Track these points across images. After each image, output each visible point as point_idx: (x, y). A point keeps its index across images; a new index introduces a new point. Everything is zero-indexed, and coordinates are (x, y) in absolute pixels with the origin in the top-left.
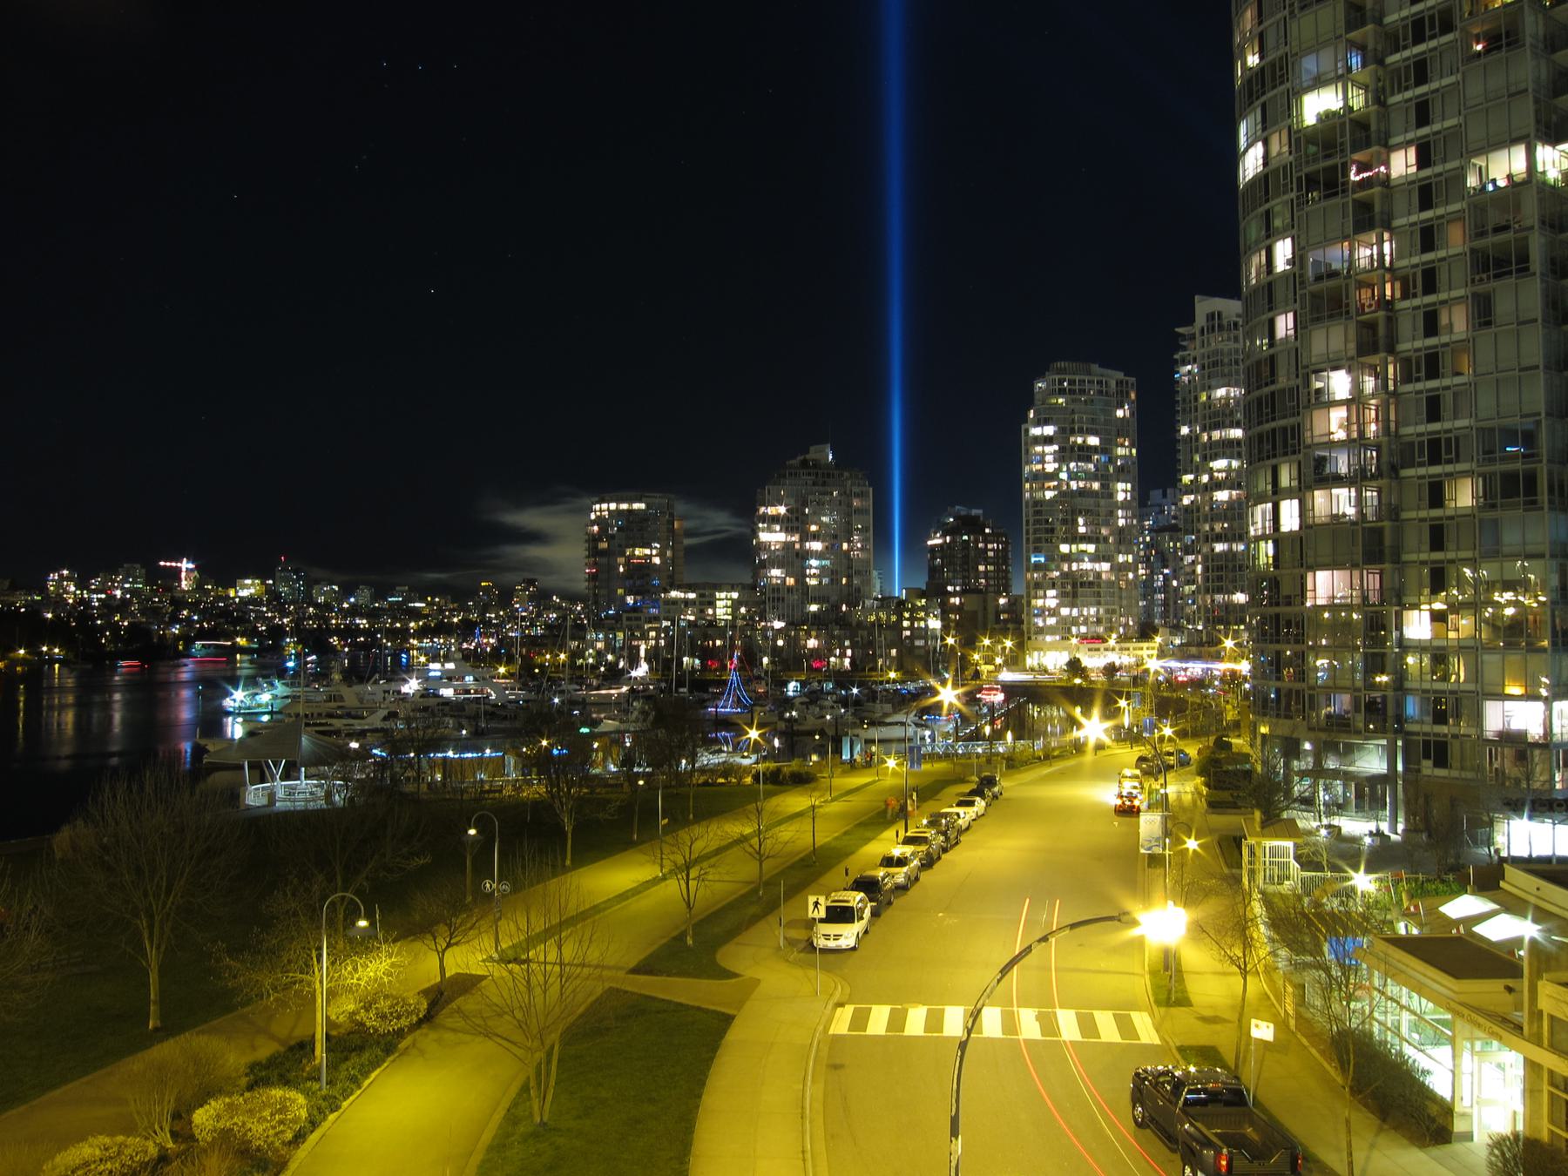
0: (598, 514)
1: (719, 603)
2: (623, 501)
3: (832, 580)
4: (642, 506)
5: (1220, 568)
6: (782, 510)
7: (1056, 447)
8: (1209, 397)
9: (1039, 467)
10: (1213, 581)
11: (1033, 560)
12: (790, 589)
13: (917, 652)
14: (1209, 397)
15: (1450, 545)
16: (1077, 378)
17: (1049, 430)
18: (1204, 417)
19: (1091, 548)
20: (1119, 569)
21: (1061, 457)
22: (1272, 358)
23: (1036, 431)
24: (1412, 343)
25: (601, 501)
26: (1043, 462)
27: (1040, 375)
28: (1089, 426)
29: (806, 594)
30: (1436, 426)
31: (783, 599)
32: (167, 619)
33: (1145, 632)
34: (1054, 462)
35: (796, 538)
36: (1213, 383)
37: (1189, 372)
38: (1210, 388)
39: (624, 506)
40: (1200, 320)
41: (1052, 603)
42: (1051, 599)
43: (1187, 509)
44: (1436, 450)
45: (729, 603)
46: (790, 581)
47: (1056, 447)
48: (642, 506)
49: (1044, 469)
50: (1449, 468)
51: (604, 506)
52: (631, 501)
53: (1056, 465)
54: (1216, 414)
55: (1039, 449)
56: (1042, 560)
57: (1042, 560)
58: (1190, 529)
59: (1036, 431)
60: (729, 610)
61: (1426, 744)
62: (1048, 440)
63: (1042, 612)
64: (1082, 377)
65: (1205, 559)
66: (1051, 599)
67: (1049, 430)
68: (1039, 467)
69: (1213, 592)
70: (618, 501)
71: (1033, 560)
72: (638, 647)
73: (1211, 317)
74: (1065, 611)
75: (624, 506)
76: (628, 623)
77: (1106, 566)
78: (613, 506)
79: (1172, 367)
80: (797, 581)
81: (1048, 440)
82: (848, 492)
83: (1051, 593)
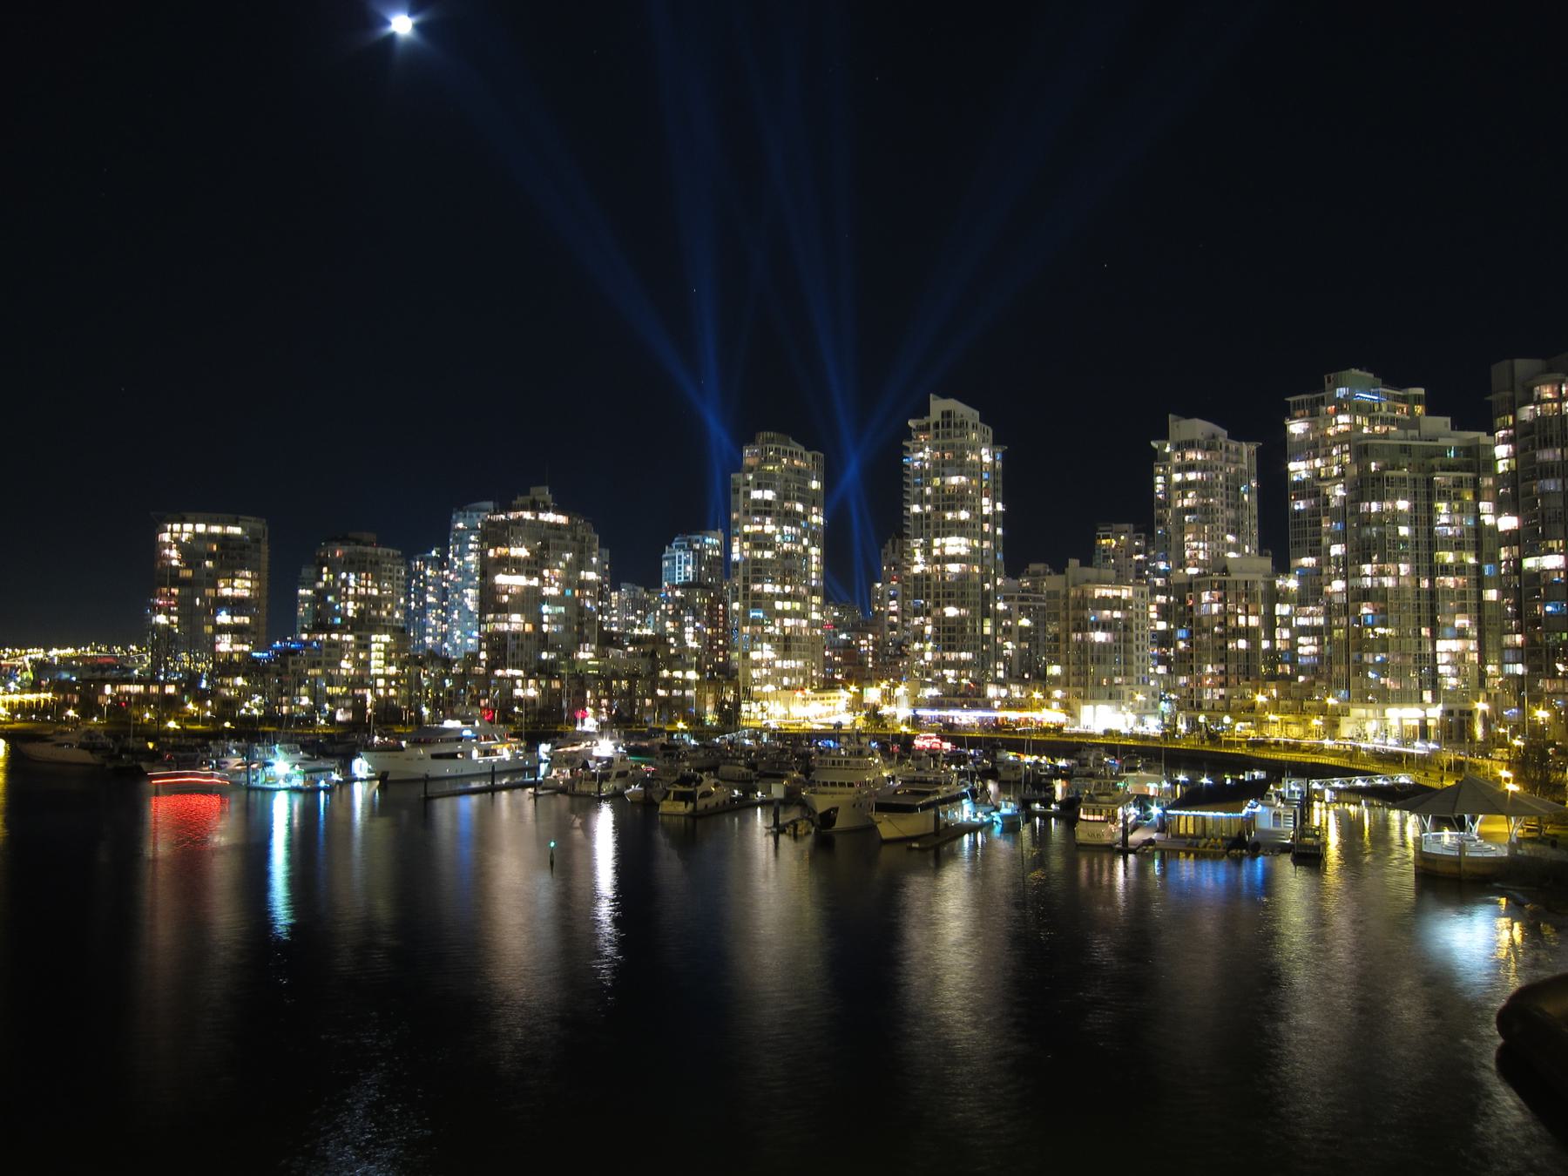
0: (175, 535)
1: (374, 647)
2: (216, 523)
3: (566, 627)
4: (237, 530)
5: (949, 630)
6: (521, 552)
8: (943, 483)
9: (759, 528)
10: (943, 640)
11: (752, 615)
12: (528, 636)
13: (674, 702)
14: (943, 483)
19: (779, 605)
20: (813, 625)
25: (183, 521)
27: (751, 441)
29: (544, 641)
31: (522, 646)
32: (1000, 674)
33: (829, 685)
35: (535, 582)
36: (947, 470)
37: (922, 459)
38: (943, 474)
39: (216, 529)
40: (935, 414)
42: (765, 652)
43: (916, 577)
45: (382, 647)
46: (529, 627)
48: (237, 530)
49: (763, 530)
51: (188, 527)
52: (224, 524)
54: (950, 498)
56: (761, 615)
57: (761, 615)
60: (382, 655)
63: (757, 665)
64: (778, 446)
65: (935, 623)
66: (765, 652)
68: (759, 528)
69: (944, 650)
70: (209, 523)
71: (752, 615)
72: (364, 698)
73: (947, 414)
74: (778, 664)
75: (216, 529)
76: (294, 667)
77: (804, 623)
78: (201, 528)
79: (901, 452)
80: (534, 627)
82: (579, 537)
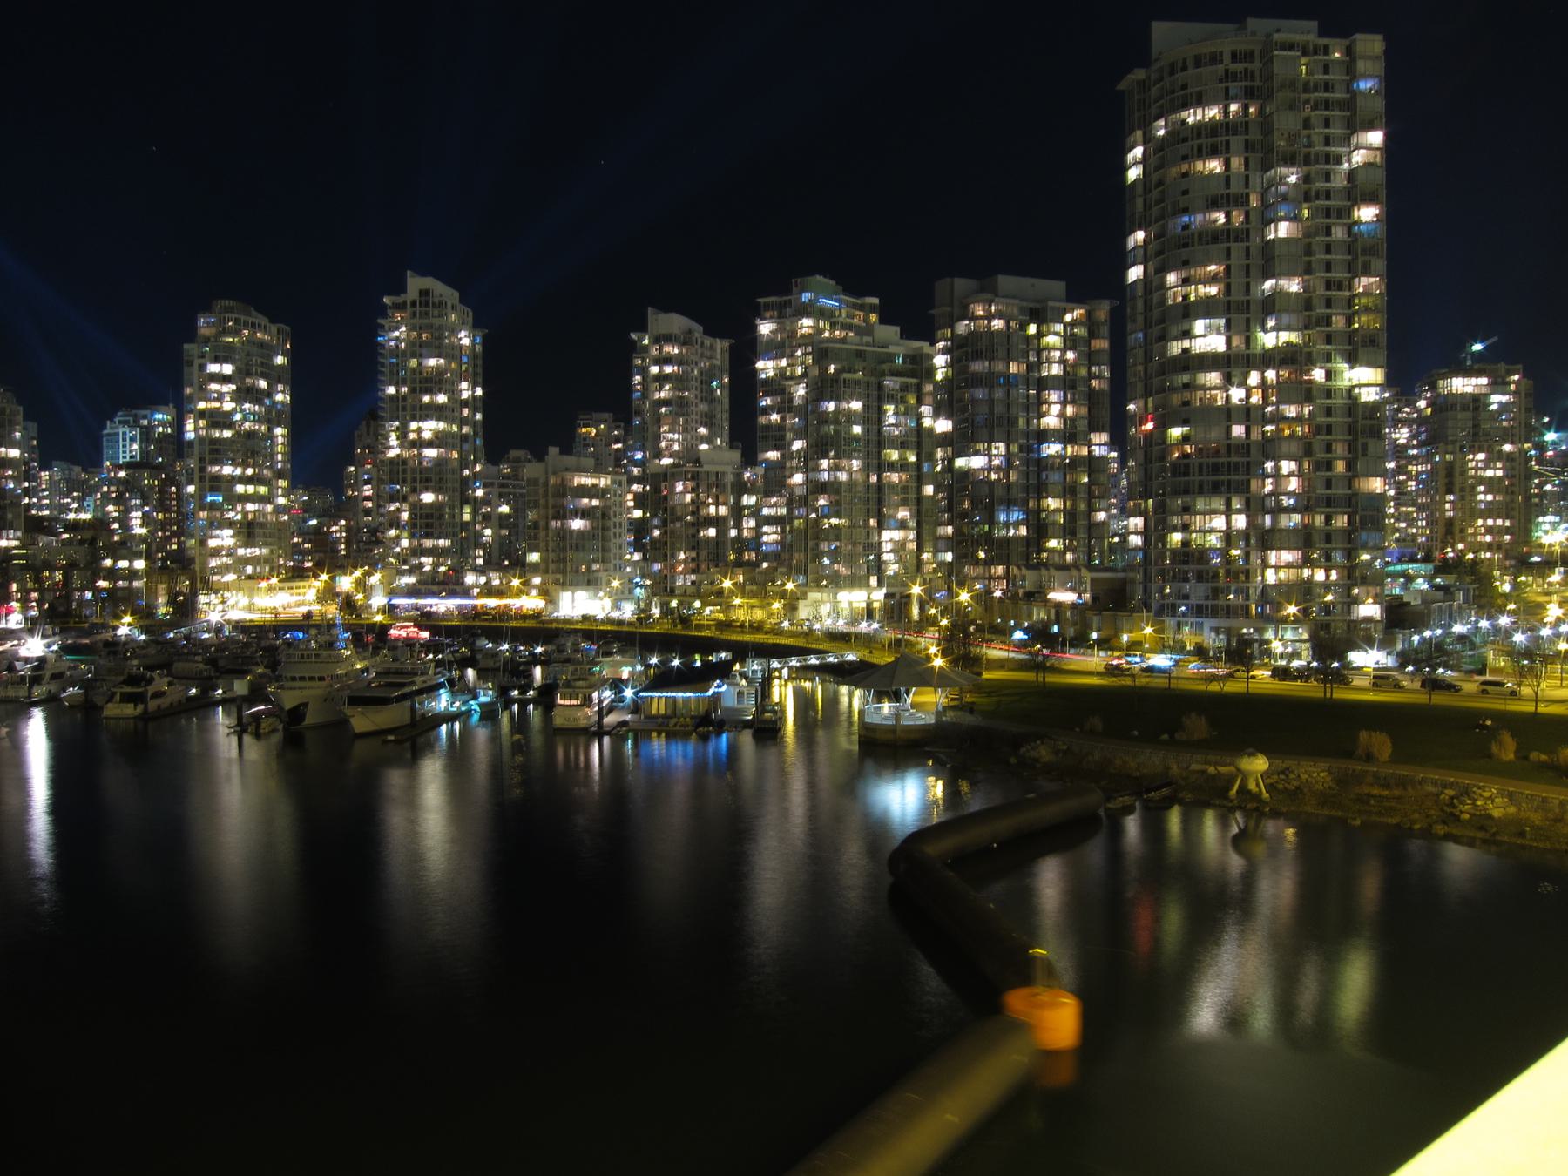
5: (427, 516)
7: (234, 387)
9: (217, 405)
10: (421, 527)
11: (210, 499)
13: (119, 594)
14: (420, 364)
15: (1333, 542)
16: (243, 318)
17: (228, 369)
18: (414, 381)
19: (240, 489)
20: (279, 510)
21: (238, 397)
22: (1248, 445)
23: (213, 368)
24: (1321, 455)
26: (220, 397)
27: (207, 309)
28: (264, 370)
30: (1329, 492)
32: (480, 561)
33: (298, 574)
34: (232, 401)
36: (424, 351)
37: (397, 339)
38: (421, 356)
40: (412, 292)
41: (230, 542)
42: (224, 538)
43: (392, 461)
44: (1329, 502)
47: (234, 387)
50: (1334, 510)
53: (234, 405)
54: (427, 380)
55: (214, 386)
56: (221, 499)
58: (396, 480)
59: (213, 368)
61: (1322, 625)
62: (224, 379)
63: (216, 552)
66: (224, 538)
67: (228, 369)
68: (217, 405)
69: (422, 537)
73: (424, 293)
74: (241, 552)
77: (269, 508)
79: (376, 330)
81: (224, 379)
83: (229, 532)
